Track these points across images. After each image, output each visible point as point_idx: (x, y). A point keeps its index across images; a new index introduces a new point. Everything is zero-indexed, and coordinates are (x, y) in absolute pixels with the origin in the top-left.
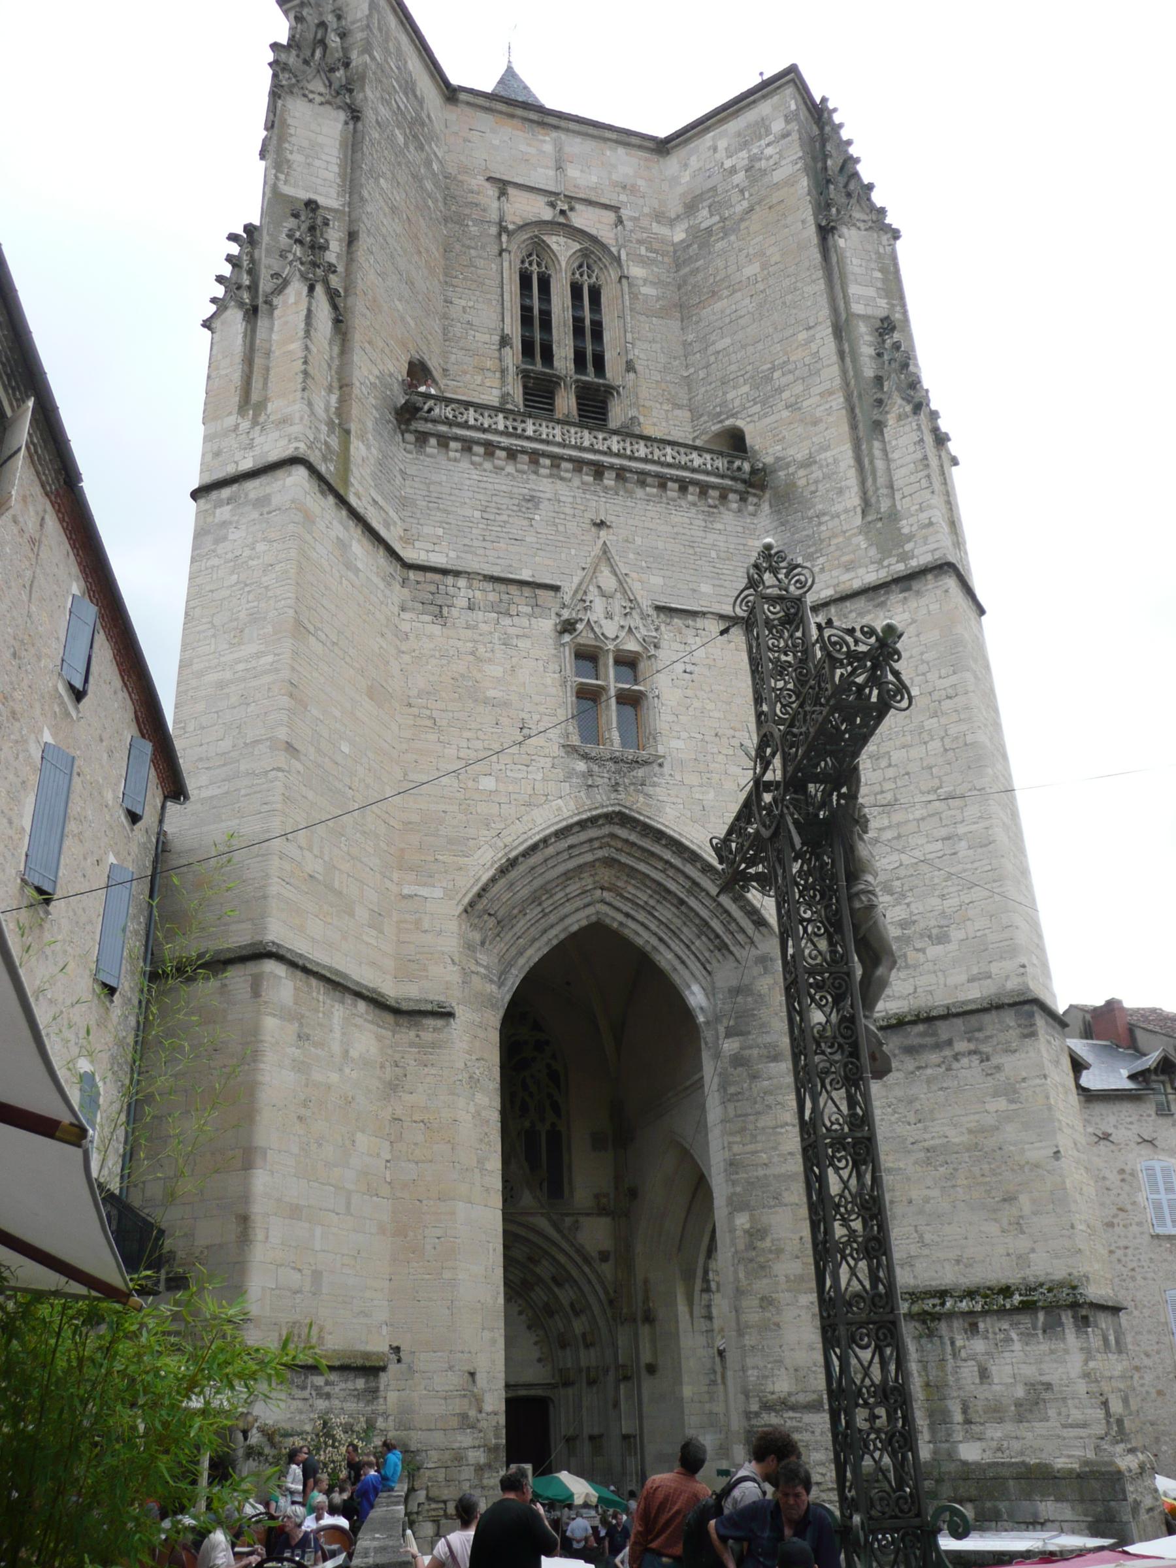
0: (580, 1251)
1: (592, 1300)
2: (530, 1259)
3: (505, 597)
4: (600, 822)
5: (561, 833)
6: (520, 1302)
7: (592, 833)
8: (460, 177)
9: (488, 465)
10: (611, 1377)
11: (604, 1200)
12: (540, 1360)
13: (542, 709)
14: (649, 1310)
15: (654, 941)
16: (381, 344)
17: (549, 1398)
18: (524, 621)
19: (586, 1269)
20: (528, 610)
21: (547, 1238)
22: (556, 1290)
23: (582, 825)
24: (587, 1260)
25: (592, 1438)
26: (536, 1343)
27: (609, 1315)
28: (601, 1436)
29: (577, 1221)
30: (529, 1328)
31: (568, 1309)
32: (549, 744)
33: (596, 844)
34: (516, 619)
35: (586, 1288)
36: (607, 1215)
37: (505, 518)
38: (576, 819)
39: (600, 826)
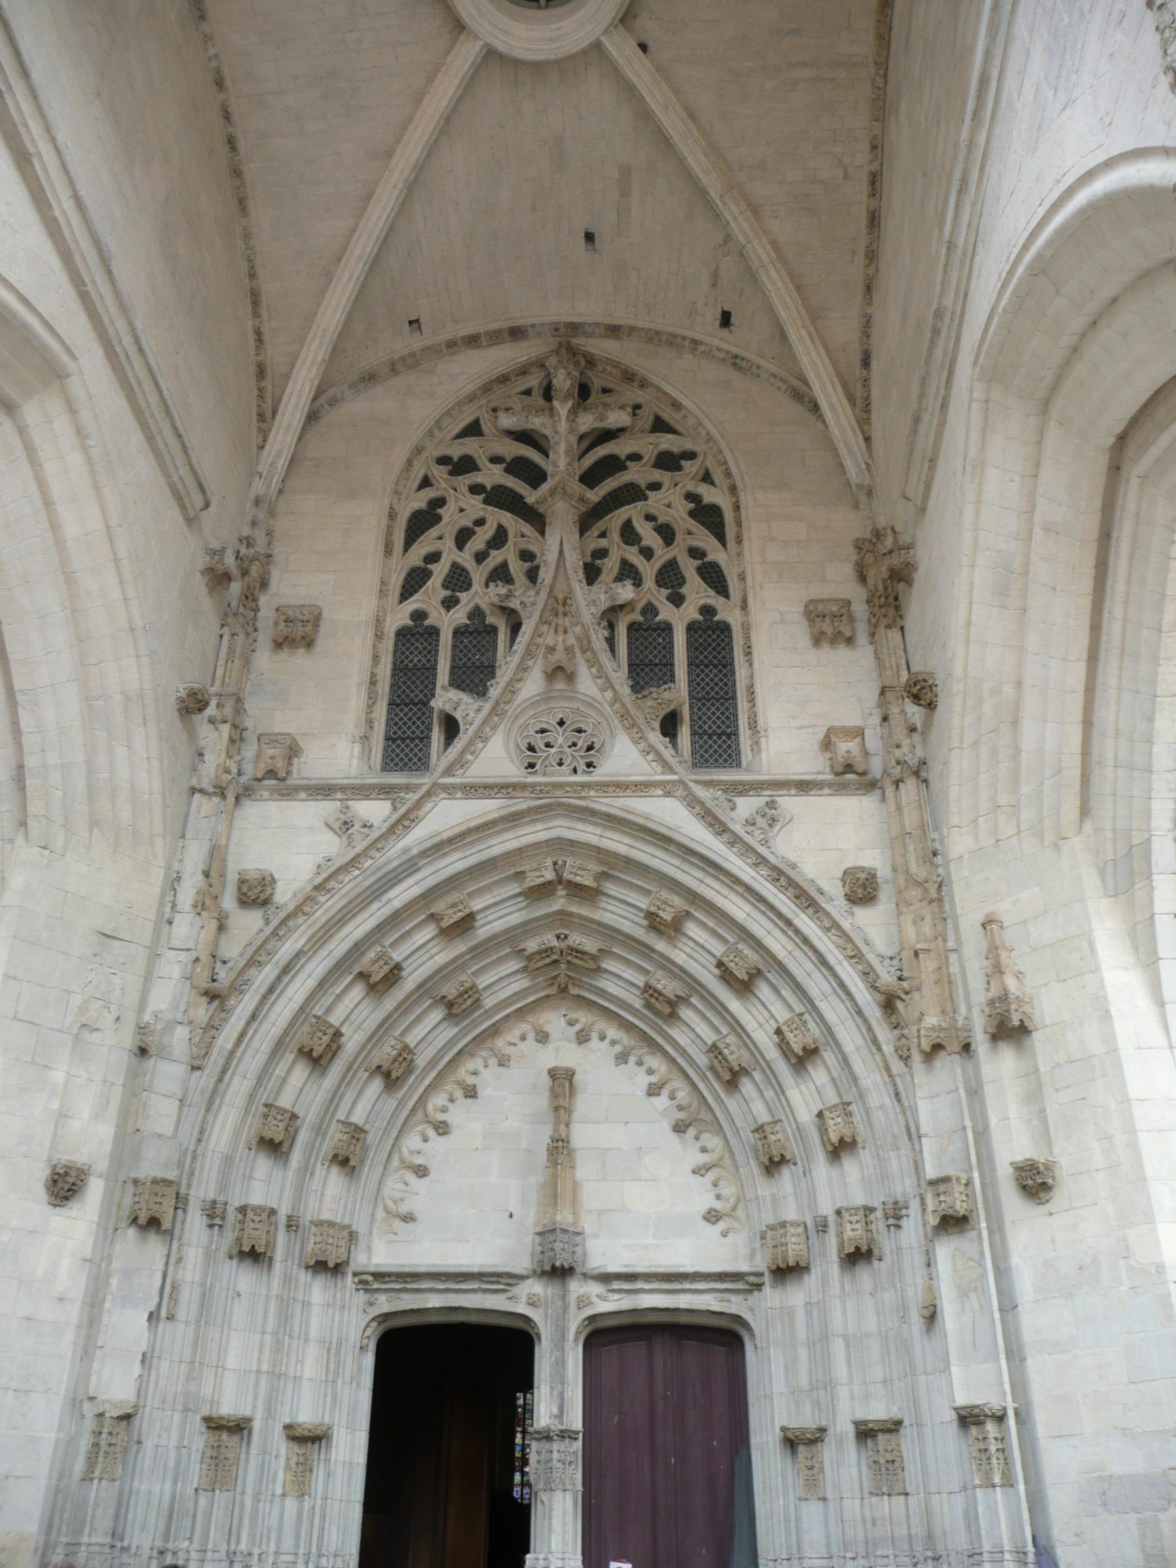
0: (780, 875)
1: (834, 1011)
2: (654, 922)
6: (654, 1061)
10: (913, 1229)
11: (846, 747)
12: (712, 1217)
14: (1004, 998)
17: (738, 1319)
19: (805, 923)
21: (687, 853)
22: (734, 1005)
24: (806, 899)
25: (865, 1433)
26: (699, 1171)
27: (888, 1049)
28: (894, 1427)
29: (771, 805)
30: (679, 1128)
31: (772, 1053)
35: (816, 984)
36: (870, 785)
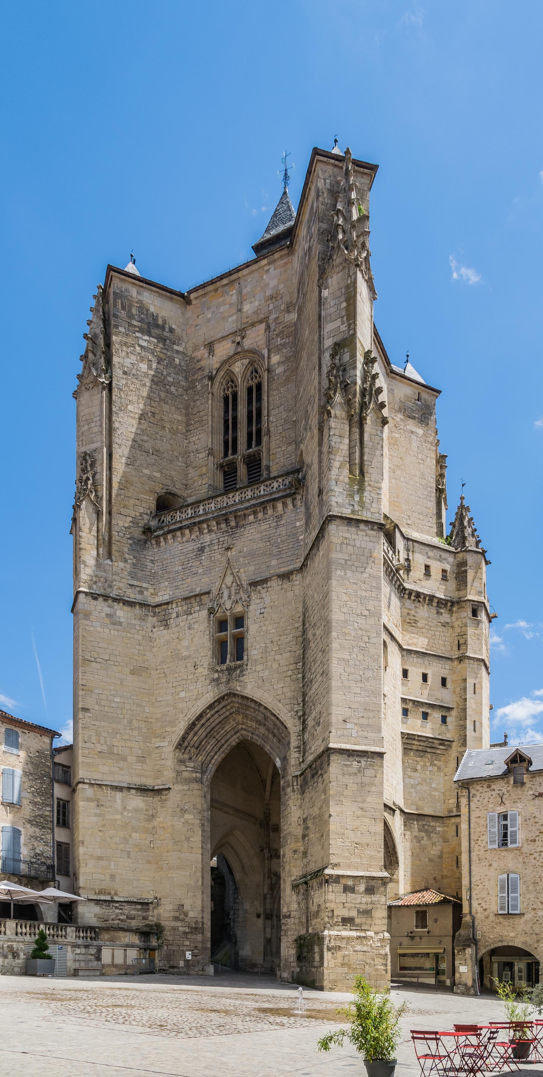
3: (189, 605)
4: (226, 698)
5: (211, 707)
7: (223, 704)
8: (193, 356)
9: (185, 539)
13: (202, 654)
15: (263, 742)
16: (132, 502)
18: (196, 615)
20: (197, 608)
23: (219, 701)
32: (203, 671)
33: (228, 707)
34: (193, 615)
37: (190, 564)
38: (213, 701)
39: (227, 700)
